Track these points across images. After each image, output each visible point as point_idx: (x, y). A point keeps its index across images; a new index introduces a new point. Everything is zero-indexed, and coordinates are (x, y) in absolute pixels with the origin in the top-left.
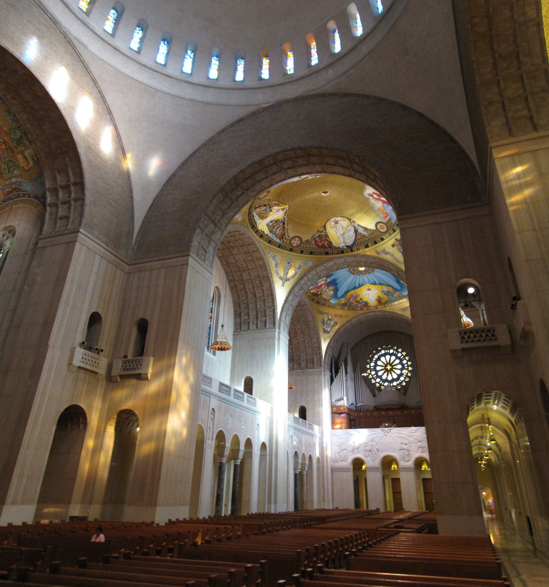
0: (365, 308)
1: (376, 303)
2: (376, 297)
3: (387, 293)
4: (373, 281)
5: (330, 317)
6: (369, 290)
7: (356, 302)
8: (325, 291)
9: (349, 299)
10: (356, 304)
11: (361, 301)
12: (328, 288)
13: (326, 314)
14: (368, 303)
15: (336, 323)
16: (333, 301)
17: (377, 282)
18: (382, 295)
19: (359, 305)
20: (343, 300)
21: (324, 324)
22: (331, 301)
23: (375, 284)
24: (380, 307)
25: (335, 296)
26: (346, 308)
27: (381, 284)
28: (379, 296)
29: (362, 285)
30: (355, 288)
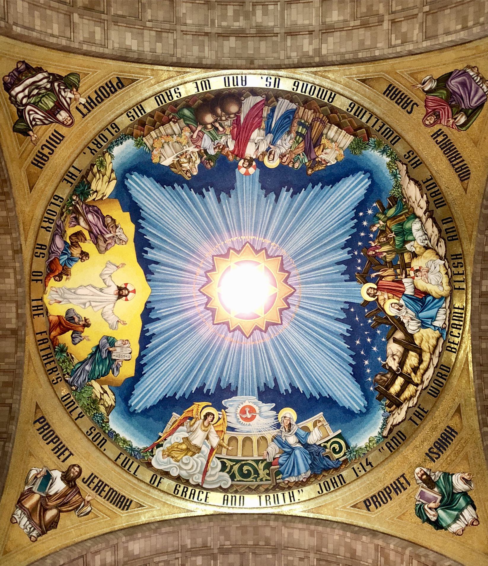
0: (40, 265)
1: (57, 310)
2: (82, 312)
3: (103, 356)
4: (163, 312)
5: (63, 115)
6: (122, 293)
7: (78, 234)
8: (195, 142)
9: (97, 212)
10: (70, 231)
11: (76, 252)
12: (203, 153)
13: (91, 104)
14: (59, 278)
15: (25, 132)
16: (124, 151)
17: (154, 328)
18: (92, 338)
19: (59, 242)
20: (103, 186)
21: (54, 78)
22: (129, 143)
23: (148, 315)
24: (41, 324)
25: (144, 166)
26: (65, 192)
27: (145, 339)
28: (87, 325)
29: (147, 272)
30: (142, 244)
